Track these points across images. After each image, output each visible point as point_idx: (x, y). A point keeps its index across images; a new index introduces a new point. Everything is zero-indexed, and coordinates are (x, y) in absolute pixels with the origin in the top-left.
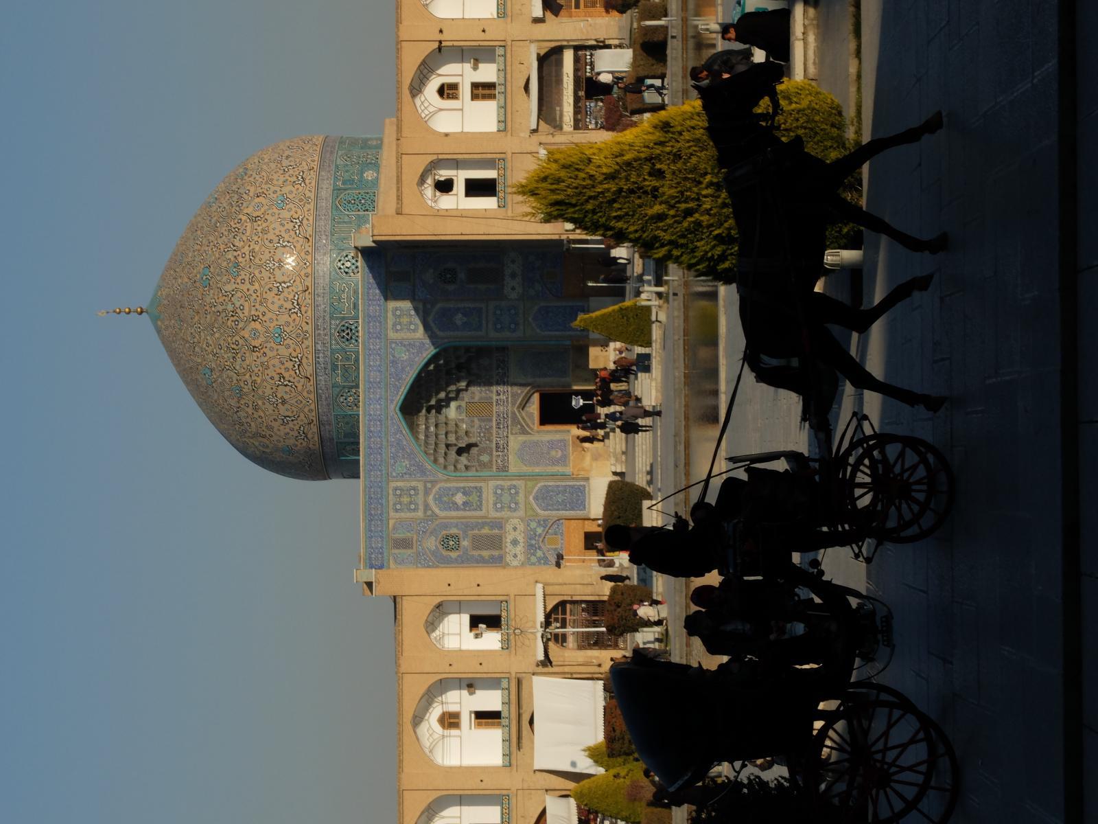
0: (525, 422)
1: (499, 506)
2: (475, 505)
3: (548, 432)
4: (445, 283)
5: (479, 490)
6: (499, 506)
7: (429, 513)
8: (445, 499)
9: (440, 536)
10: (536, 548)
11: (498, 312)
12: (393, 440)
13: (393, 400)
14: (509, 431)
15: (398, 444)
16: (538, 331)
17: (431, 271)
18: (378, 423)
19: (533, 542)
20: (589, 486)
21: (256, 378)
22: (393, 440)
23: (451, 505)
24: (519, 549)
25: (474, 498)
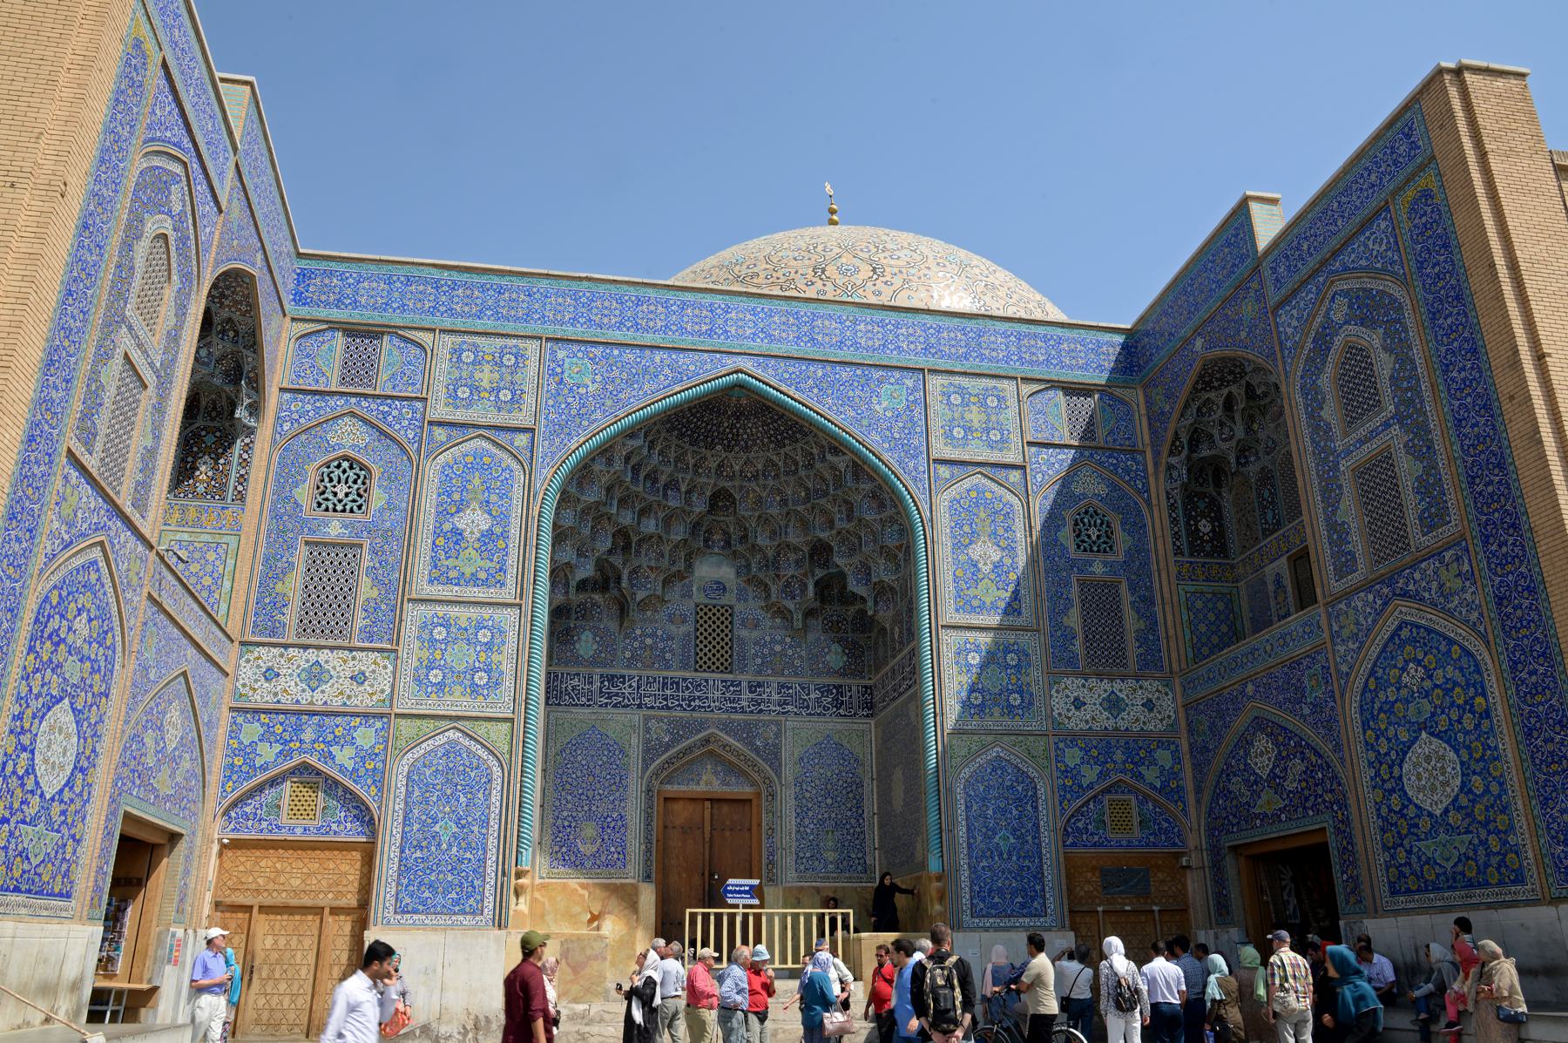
0: (677, 756)
1: (440, 633)
2: (450, 562)
3: (649, 817)
4: (1076, 524)
5: (494, 578)
6: (440, 633)
7: (440, 434)
8: (477, 482)
9: (364, 460)
10: (286, 742)
11: (1012, 659)
12: (658, 359)
13: (765, 369)
14: (652, 712)
15: (646, 371)
16: (966, 773)
17: (1103, 490)
18: (704, 328)
19: (308, 735)
20: (476, 927)
21: (762, 276)
22: (658, 359)
23: (456, 496)
24: (292, 691)
25: (471, 561)
